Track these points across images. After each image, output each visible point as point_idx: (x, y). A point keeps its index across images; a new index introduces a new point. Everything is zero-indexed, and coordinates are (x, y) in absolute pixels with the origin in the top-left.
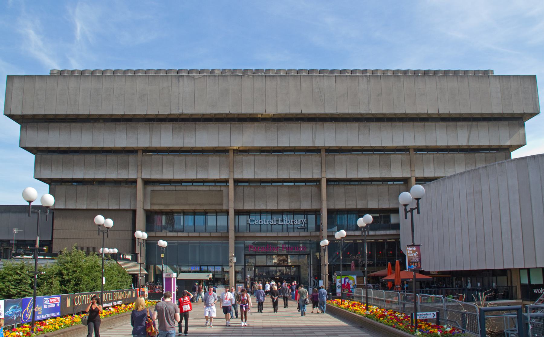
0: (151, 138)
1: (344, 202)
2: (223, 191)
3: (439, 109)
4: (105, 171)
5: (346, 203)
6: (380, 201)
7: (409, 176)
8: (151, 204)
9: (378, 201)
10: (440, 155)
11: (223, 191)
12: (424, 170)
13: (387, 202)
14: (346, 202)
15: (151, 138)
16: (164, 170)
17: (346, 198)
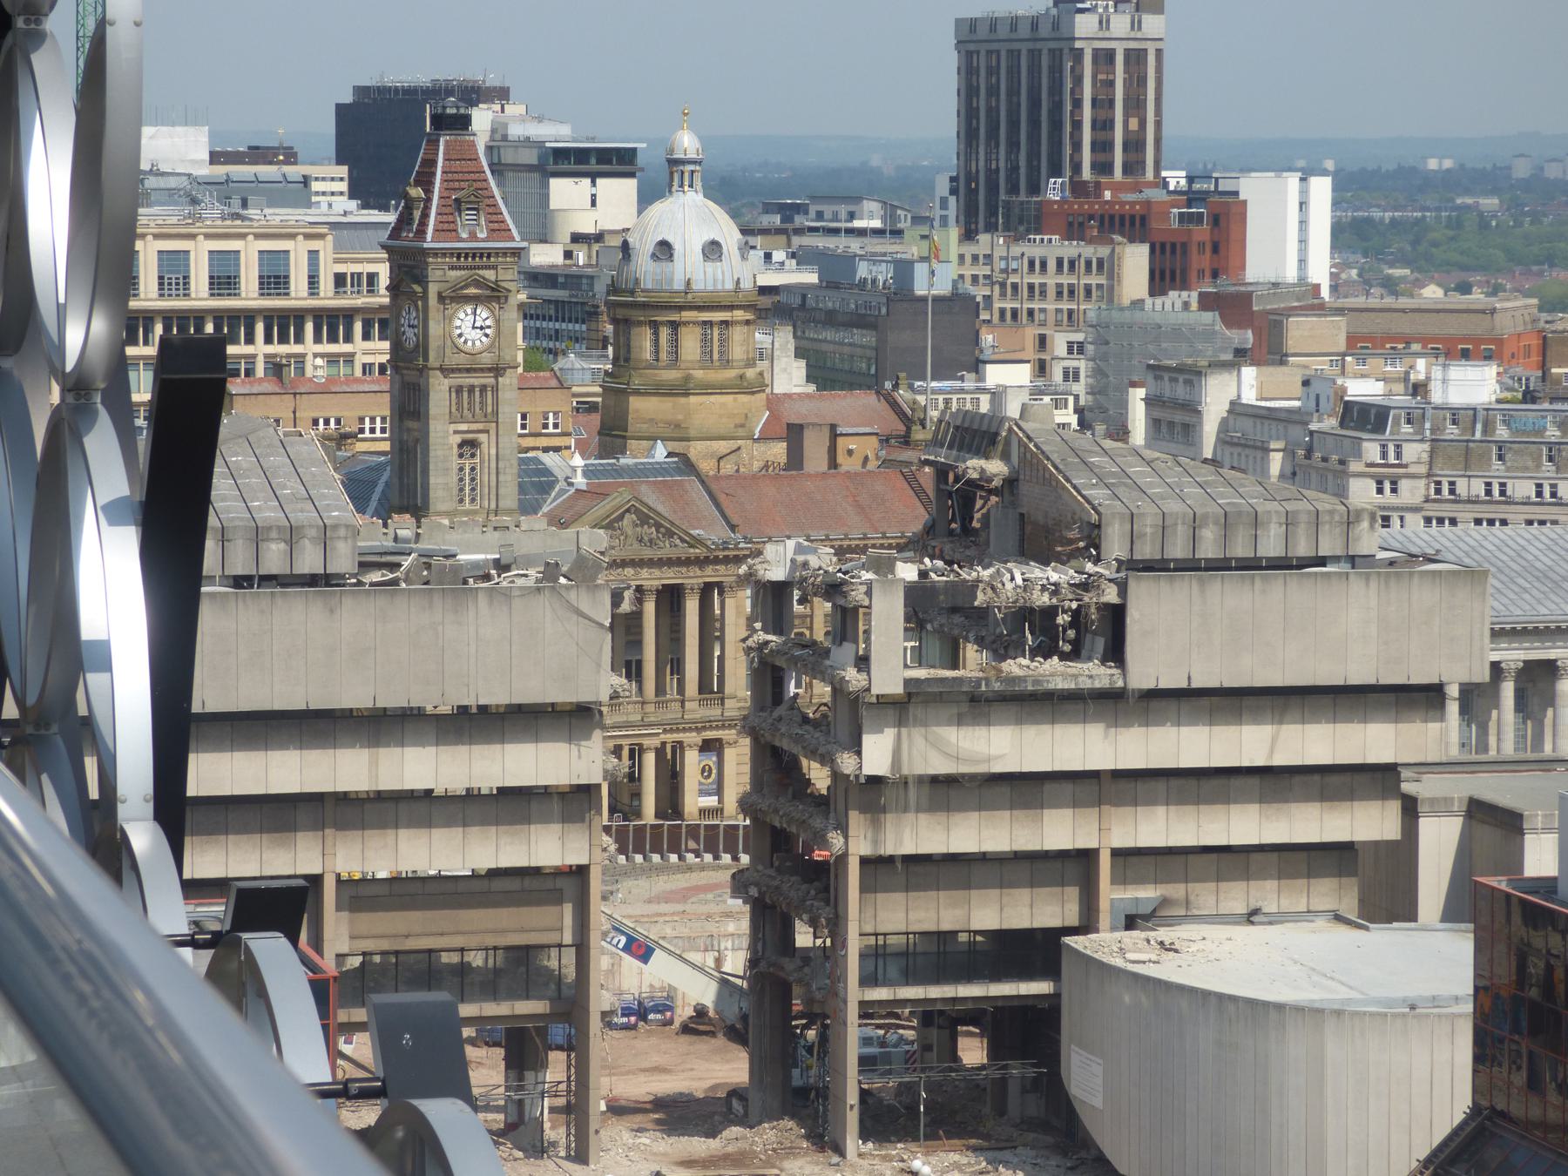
0: (374, 764)
1: (904, 915)
2: (561, 890)
3: (1192, 677)
4: (225, 853)
5: (910, 917)
6: (1005, 910)
7: (1092, 844)
8: (352, 937)
9: (1001, 909)
10: (1192, 783)
11: (561, 890)
12: (1139, 828)
13: (1026, 911)
14: (910, 913)
15: (374, 764)
16: (403, 846)
17: (910, 903)
